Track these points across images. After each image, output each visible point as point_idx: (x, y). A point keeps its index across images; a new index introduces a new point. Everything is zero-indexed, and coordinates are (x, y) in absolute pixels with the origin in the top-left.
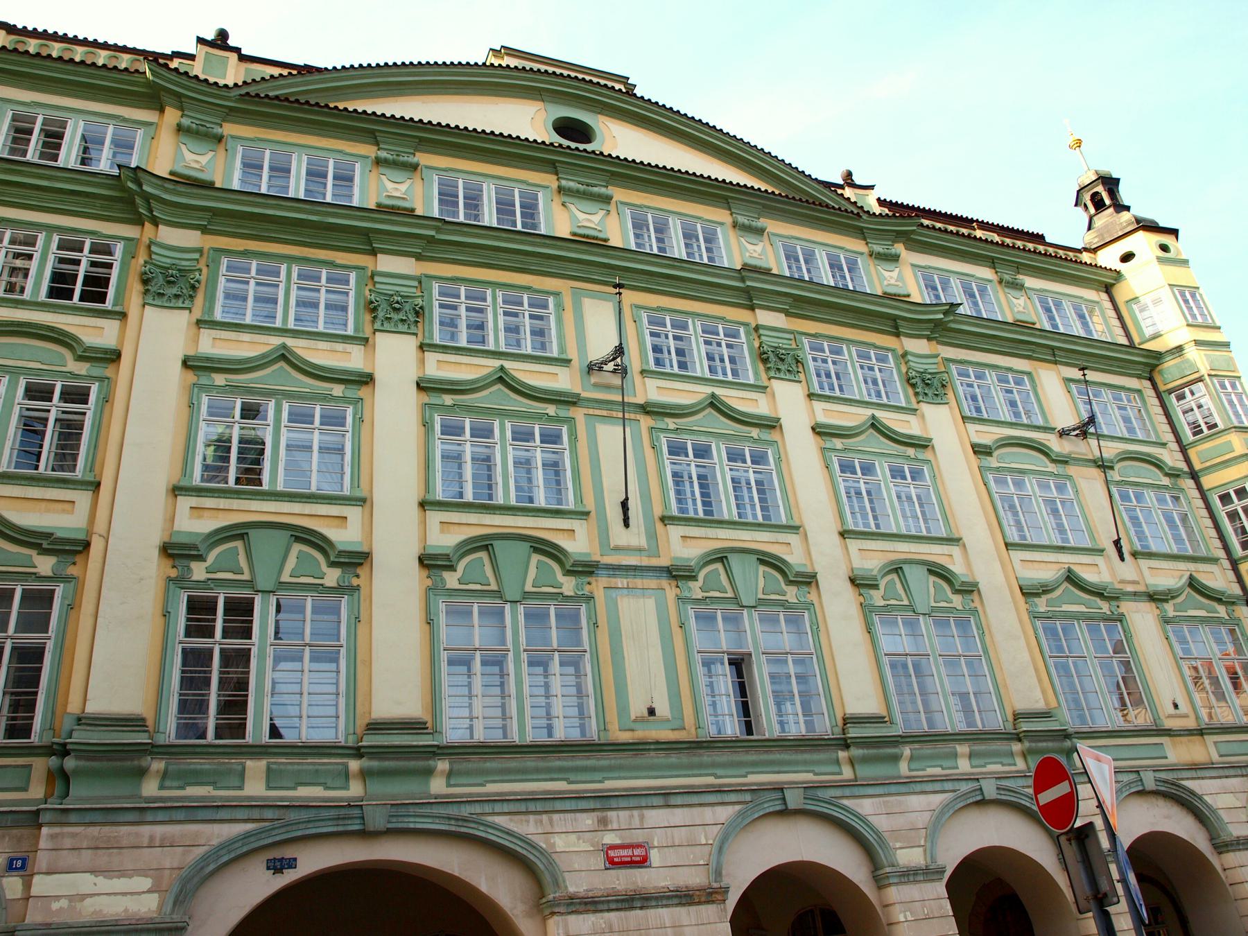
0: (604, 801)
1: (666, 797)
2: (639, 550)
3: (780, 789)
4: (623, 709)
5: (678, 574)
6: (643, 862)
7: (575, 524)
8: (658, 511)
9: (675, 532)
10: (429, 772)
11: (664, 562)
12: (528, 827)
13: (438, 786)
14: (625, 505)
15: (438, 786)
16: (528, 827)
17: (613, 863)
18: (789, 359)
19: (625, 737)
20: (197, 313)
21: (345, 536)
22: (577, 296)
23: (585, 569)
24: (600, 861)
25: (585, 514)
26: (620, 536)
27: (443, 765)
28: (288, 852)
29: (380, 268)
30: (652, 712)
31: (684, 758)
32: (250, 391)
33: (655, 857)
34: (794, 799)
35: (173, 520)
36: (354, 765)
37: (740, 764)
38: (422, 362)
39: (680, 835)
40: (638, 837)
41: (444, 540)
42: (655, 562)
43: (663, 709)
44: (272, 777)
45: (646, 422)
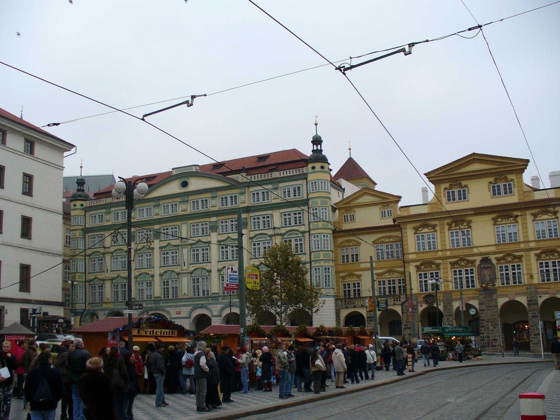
0: (176, 306)
1: (184, 306)
2: (186, 270)
3: (198, 304)
4: (182, 294)
5: (191, 273)
6: (180, 314)
7: (178, 267)
8: (189, 263)
9: (191, 266)
10: (160, 303)
11: (189, 271)
12: (168, 309)
13: (161, 304)
14: (184, 263)
15: (161, 304)
16: (168, 309)
17: (177, 314)
18: (215, 228)
19: (181, 297)
20: (135, 242)
21: (151, 273)
22: (182, 224)
23: (178, 274)
24: (176, 313)
25: (179, 265)
26: (184, 268)
27: (161, 302)
28: (148, 312)
29: (155, 228)
30: (185, 294)
31: (188, 300)
32: (141, 253)
33: (182, 313)
34: (200, 306)
35: (135, 273)
36: (153, 302)
37: (195, 301)
38: (160, 243)
39: (185, 310)
40: (180, 310)
41: (162, 272)
42: (188, 271)
43: (186, 293)
44: (146, 304)
45: (190, 247)
